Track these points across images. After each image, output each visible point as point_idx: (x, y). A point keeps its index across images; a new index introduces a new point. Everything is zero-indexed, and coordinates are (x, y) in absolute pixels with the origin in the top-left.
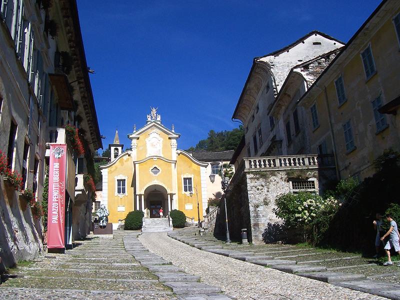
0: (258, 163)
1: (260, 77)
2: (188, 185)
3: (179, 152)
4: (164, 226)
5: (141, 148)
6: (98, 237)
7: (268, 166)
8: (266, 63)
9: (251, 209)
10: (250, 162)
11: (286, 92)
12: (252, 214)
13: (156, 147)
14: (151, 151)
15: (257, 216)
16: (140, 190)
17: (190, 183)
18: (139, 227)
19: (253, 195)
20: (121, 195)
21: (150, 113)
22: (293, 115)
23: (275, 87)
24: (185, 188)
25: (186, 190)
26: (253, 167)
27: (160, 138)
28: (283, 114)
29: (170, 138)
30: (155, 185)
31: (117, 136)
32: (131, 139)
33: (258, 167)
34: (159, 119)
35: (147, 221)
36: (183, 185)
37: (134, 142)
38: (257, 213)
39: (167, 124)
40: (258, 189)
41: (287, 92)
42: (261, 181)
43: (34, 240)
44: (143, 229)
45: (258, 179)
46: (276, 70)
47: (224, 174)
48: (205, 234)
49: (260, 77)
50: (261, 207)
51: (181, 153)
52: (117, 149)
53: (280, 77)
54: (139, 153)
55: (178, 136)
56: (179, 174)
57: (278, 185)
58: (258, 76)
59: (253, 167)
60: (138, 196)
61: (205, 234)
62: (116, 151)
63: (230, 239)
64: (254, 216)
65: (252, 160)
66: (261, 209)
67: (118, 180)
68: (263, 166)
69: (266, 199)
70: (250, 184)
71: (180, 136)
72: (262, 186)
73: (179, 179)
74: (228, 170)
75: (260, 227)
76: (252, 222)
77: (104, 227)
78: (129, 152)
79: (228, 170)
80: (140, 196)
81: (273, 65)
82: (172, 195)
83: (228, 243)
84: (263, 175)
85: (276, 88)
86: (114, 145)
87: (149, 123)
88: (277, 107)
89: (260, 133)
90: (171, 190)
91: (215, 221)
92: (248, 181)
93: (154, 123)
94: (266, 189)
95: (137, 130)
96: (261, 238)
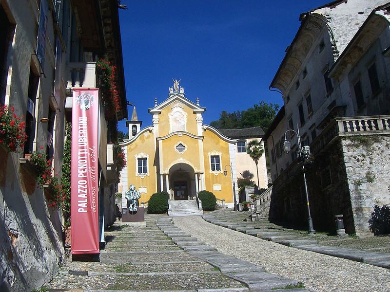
0: (355, 126)
1: (312, 35)
2: (215, 164)
3: (205, 127)
4: (192, 210)
5: (163, 124)
6: (127, 226)
7: (368, 129)
8: (321, 16)
9: (351, 187)
10: (345, 123)
11: (357, 43)
12: (353, 195)
13: (180, 123)
14: (174, 127)
15: (359, 197)
17: (218, 161)
18: (164, 210)
19: (352, 169)
20: (142, 176)
21: (172, 85)
22: (367, 72)
23: (333, 43)
24: (213, 167)
25: (213, 169)
26: (349, 130)
27: (184, 113)
28: (349, 73)
29: (194, 113)
30: (180, 164)
31: (134, 112)
32: (152, 114)
33: (355, 130)
34: (182, 91)
35: (173, 204)
36: (210, 164)
37: (155, 116)
38: (359, 193)
39: (191, 96)
40: (358, 160)
41: (358, 45)
42: (361, 149)
43: (50, 245)
44: (169, 212)
45: (357, 146)
46: (334, 24)
47: (253, 151)
48: (257, 220)
49: (310, 34)
50: (363, 185)
51: (207, 129)
52: (135, 126)
53: (338, 32)
54: (161, 129)
55: (203, 110)
56: (205, 151)
57: (384, 154)
58: (310, 34)
59: (349, 130)
60: (162, 176)
61: (257, 220)
62: (134, 129)
63: (314, 229)
64: (355, 197)
65: (347, 121)
66: (363, 187)
67: (138, 159)
68: (362, 130)
69: (368, 173)
70: (347, 153)
71: (205, 110)
72: (363, 156)
73: (205, 157)
74: (257, 147)
75: (364, 212)
76: (354, 206)
77: (135, 212)
78: (151, 128)
79: (257, 147)
80: (164, 175)
81: (330, 18)
82: (199, 174)
83: (312, 234)
84: (364, 142)
85: (335, 45)
86: (132, 122)
87: (172, 96)
88: (341, 65)
89: (309, 100)
91: (269, 203)
92: (345, 149)
93: (177, 96)
94: (368, 160)
95: (159, 104)
96: (367, 226)
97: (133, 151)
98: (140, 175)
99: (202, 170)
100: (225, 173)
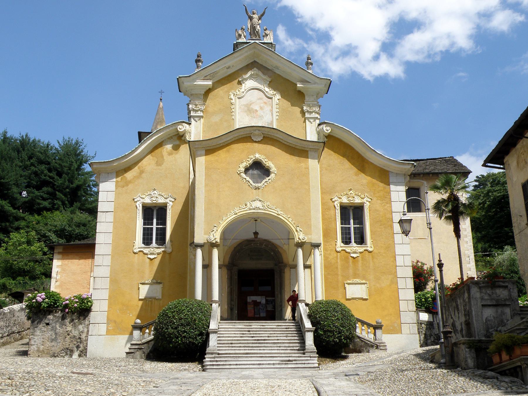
16: (207, 233)
24: (346, 233)
25: (346, 241)
90: (306, 234)
97: (130, 186)
98: (146, 251)
99: (317, 237)
100: (406, 225)
